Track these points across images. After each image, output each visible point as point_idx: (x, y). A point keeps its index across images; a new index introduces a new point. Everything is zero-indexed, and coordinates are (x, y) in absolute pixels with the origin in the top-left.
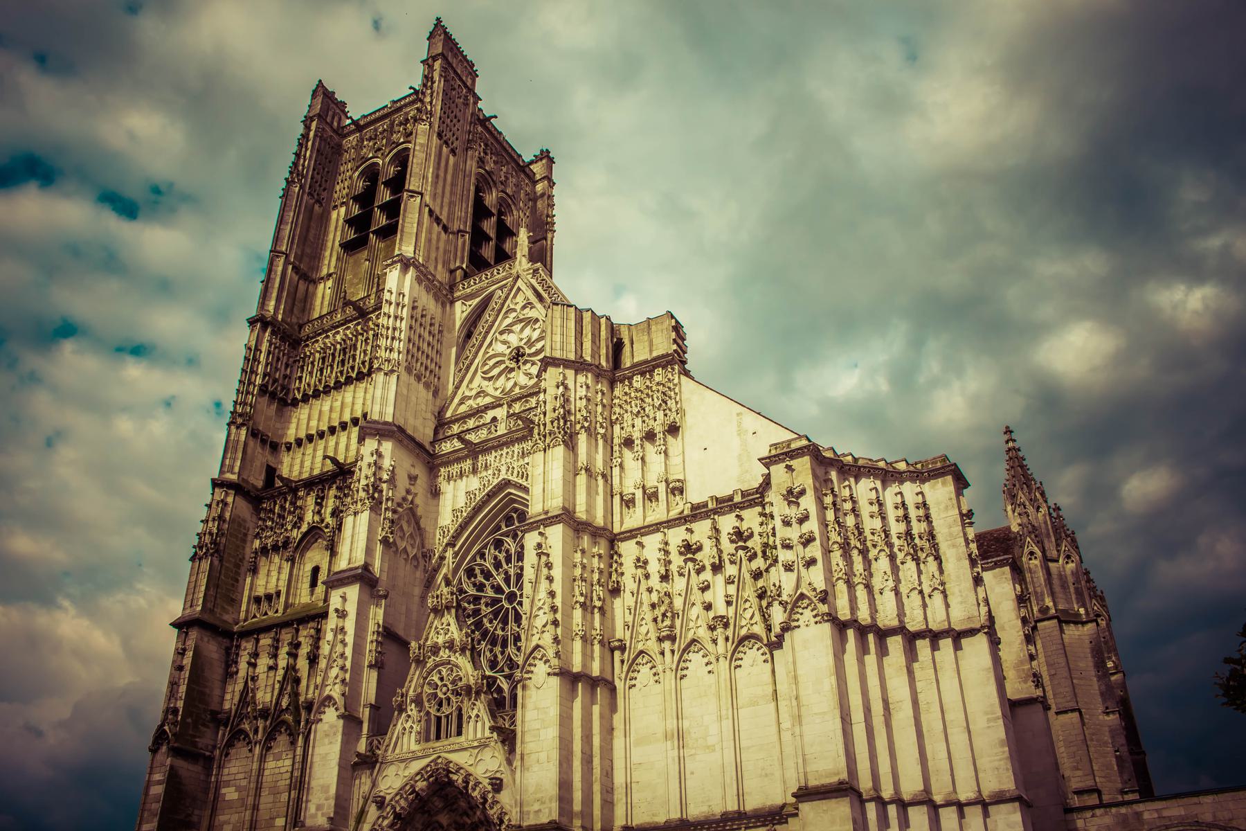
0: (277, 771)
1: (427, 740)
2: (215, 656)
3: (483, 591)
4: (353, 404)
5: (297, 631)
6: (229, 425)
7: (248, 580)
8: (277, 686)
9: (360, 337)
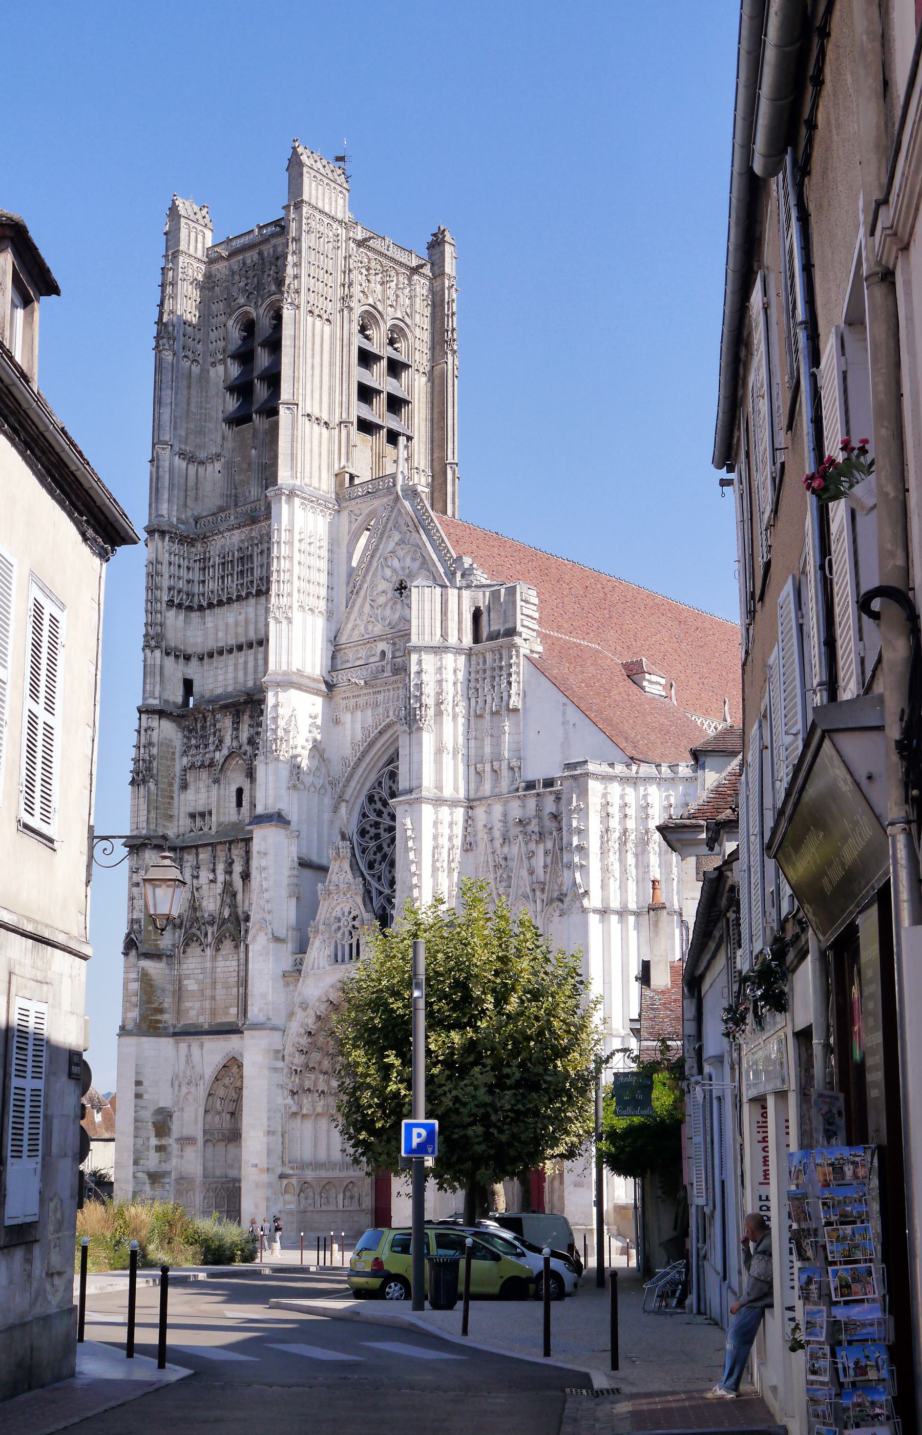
0: (226, 969)
4: (256, 622)
5: (230, 850)
6: (143, 650)
8: (218, 897)
9: (255, 548)
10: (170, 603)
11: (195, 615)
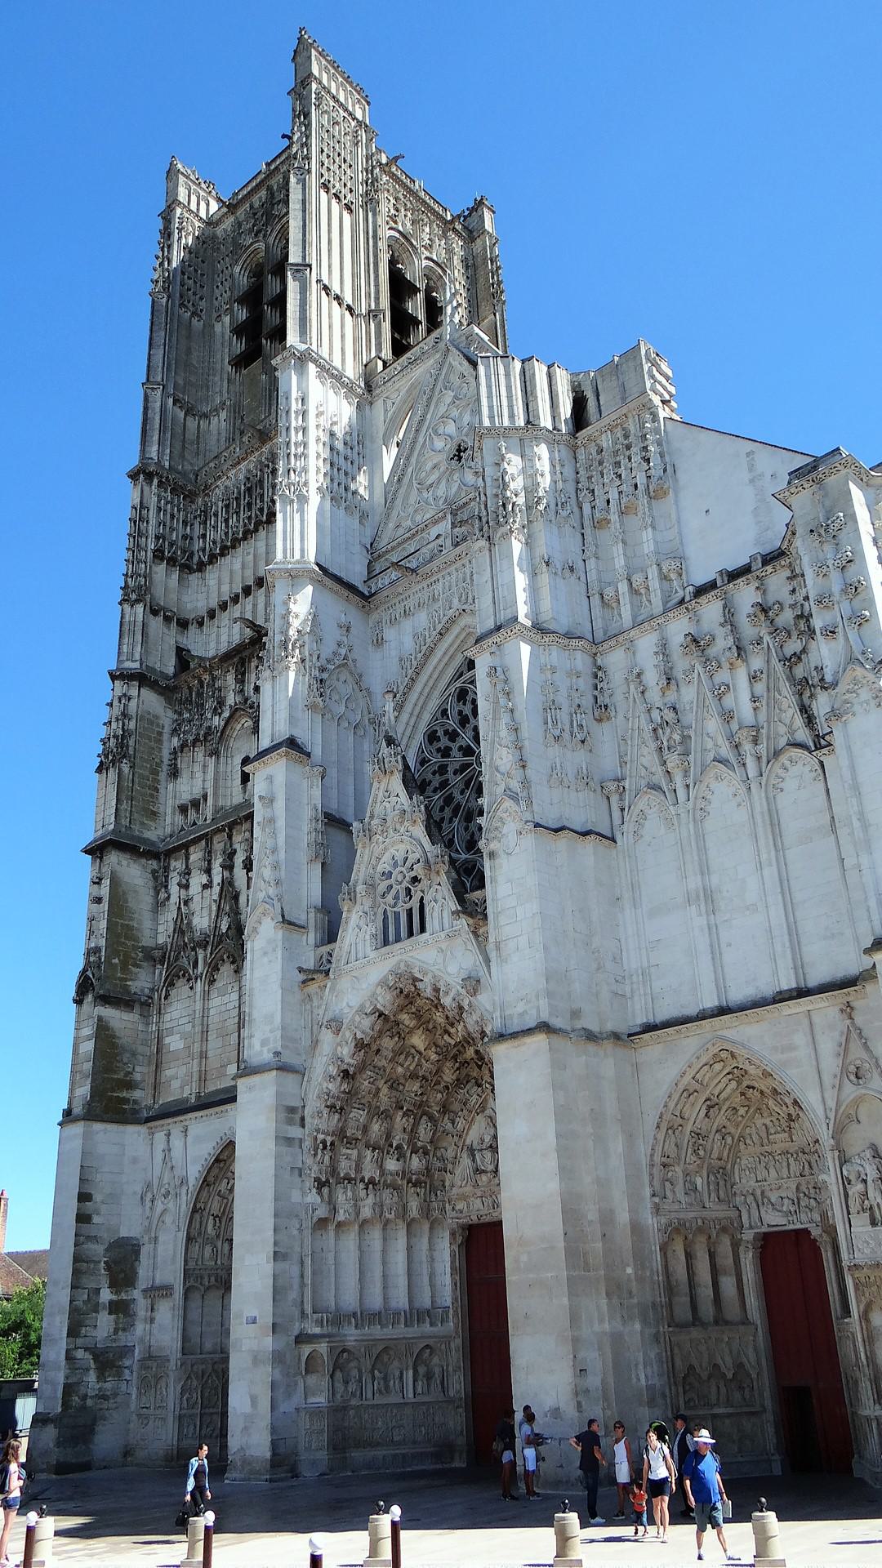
0: (223, 1008)
1: (386, 943)
2: (139, 881)
3: (449, 756)
5: (230, 837)
7: (171, 786)
9: (266, 470)
10: (158, 555)
11: (194, 578)
